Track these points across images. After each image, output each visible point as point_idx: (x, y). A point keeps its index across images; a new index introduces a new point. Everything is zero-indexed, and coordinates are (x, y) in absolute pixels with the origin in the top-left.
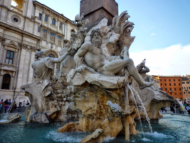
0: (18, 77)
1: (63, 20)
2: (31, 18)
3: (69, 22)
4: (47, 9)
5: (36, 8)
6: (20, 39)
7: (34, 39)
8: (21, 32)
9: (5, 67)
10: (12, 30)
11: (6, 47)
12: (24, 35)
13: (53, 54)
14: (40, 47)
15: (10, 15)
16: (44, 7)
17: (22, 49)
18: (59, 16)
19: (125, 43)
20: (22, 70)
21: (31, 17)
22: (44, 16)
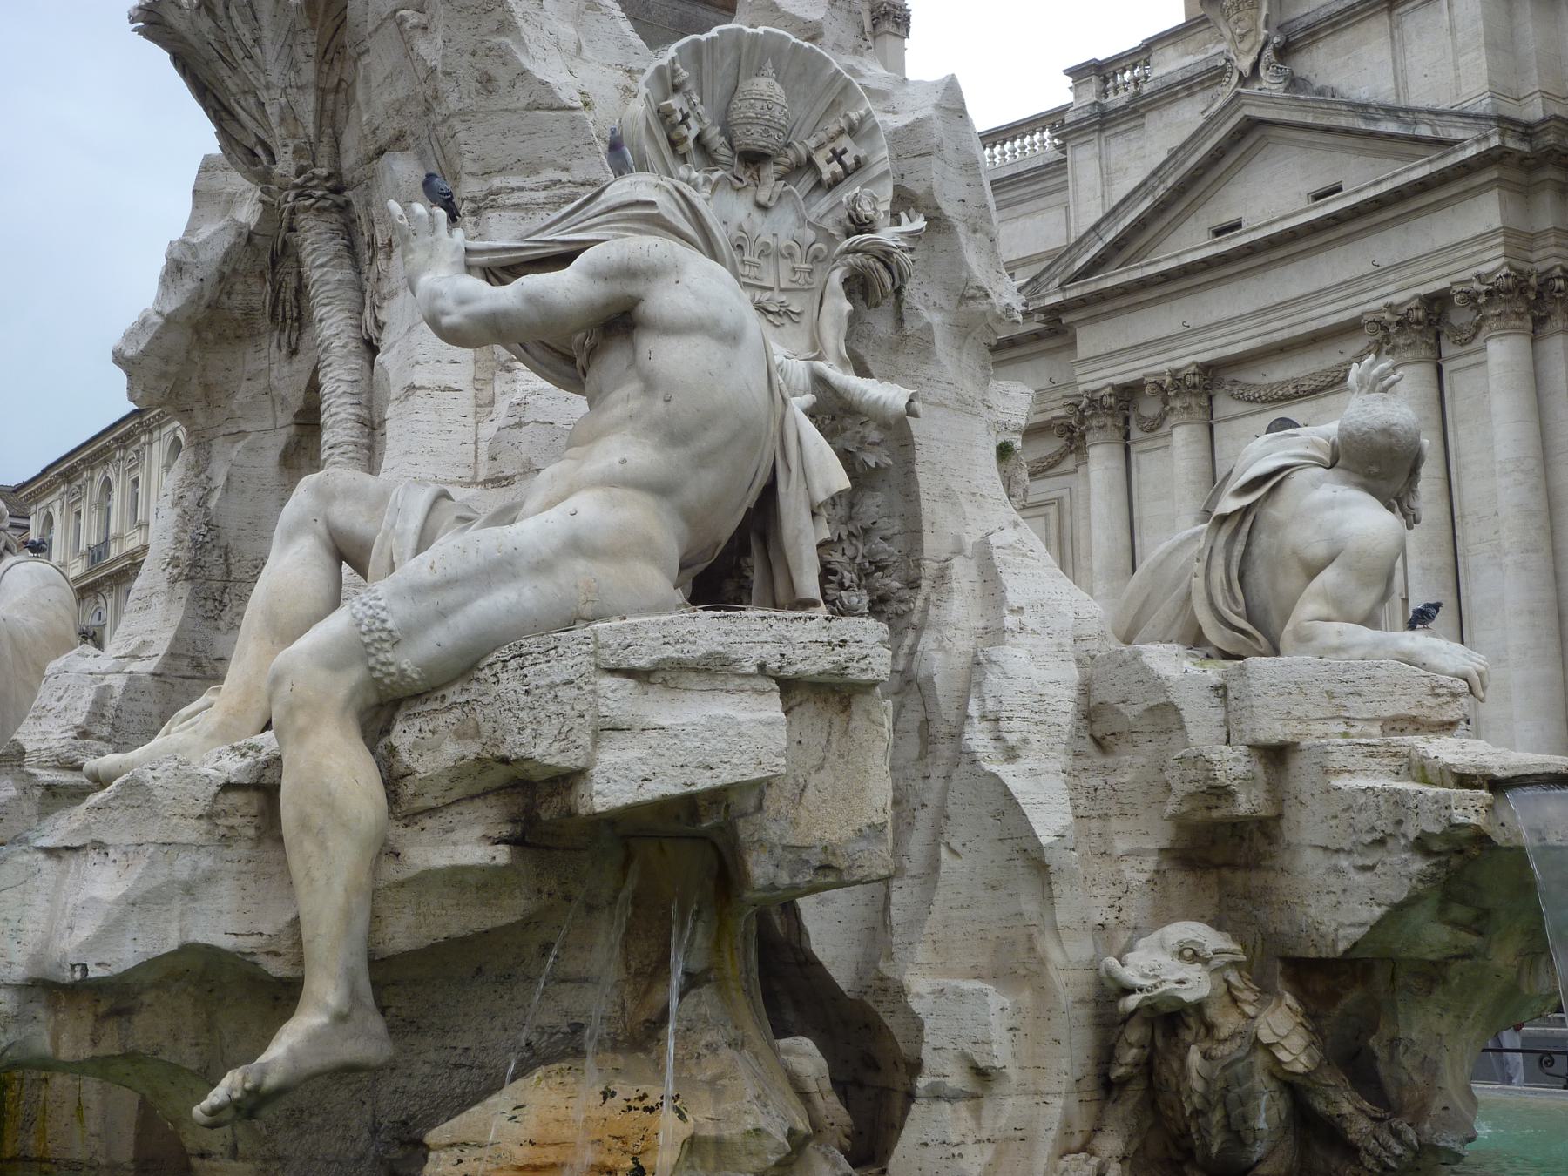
19: (383, 138)
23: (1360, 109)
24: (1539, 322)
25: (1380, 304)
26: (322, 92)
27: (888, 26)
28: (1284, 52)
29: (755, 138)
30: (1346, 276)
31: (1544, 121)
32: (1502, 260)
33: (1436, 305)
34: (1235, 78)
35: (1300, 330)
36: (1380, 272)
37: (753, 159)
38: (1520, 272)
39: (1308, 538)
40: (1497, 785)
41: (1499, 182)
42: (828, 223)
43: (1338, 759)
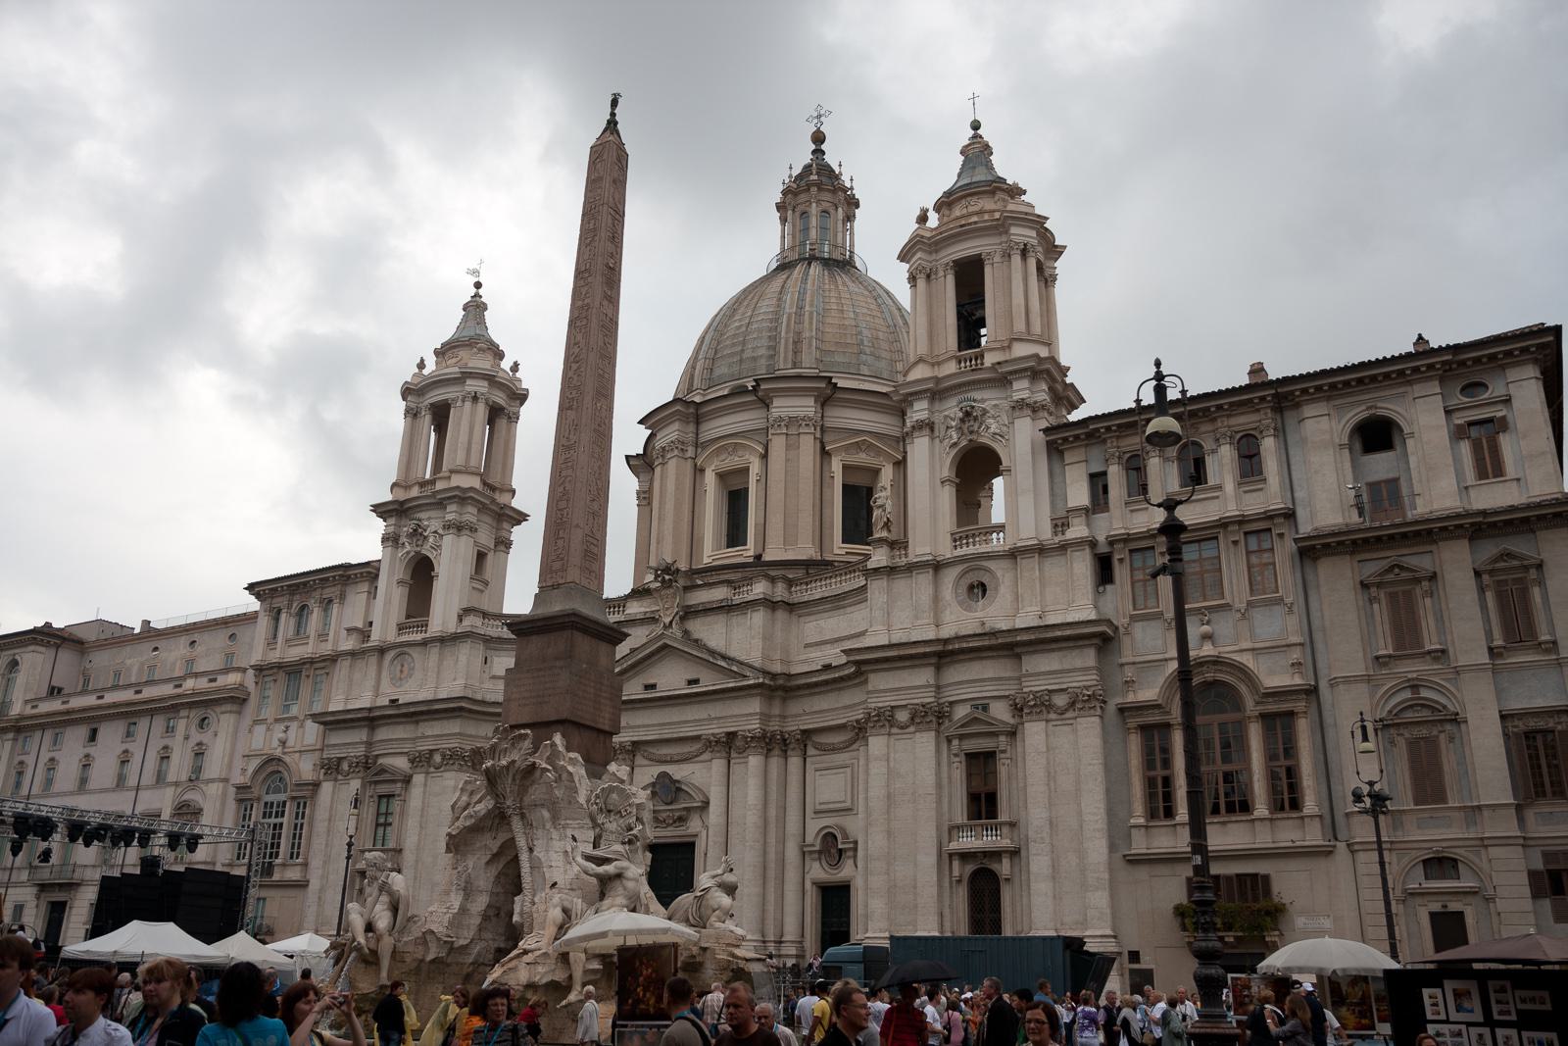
0: (1032, 877)
1: (1258, 410)
2: (1046, 534)
3: (1305, 391)
4: (1119, 426)
5: (1069, 457)
6: (1008, 674)
7: (1071, 644)
8: (993, 642)
9: (961, 840)
10: (963, 651)
11: (955, 742)
12: (1018, 650)
13: (1221, 676)
14: (1129, 672)
15: (950, 576)
16: (1097, 430)
17: (1026, 725)
18: (1208, 409)
19: (538, 803)
20: (1045, 835)
21: (1056, 525)
22: (1116, 475)
23: (712, 652)
24: (769, 750)
25: (711, 731)
26: (519, 786)
27: (502, 548)
28: (683, 619)
29: (612, 808)
30: (697, 718)
31: (780, 674)
32: (758, 725)
33: (731, 736)
34: (662, 625)
35: (675, 736)
36: (710, 719)
37: (609, 811)
38: (764, 730)
39: (714, 903)
40: (747, 960)
41: (761, 695)
42: (623, 825)
43: (717, 952)
